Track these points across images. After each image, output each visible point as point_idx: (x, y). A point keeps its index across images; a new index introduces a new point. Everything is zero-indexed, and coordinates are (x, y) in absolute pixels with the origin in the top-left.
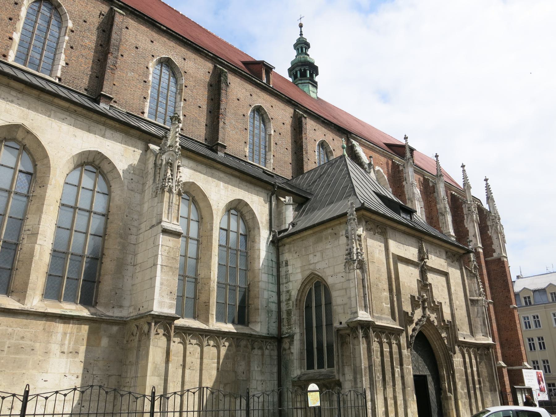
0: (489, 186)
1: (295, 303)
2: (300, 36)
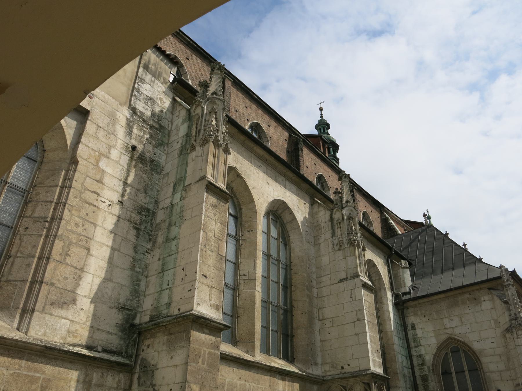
1: (431, 368)
2: (320, 119)
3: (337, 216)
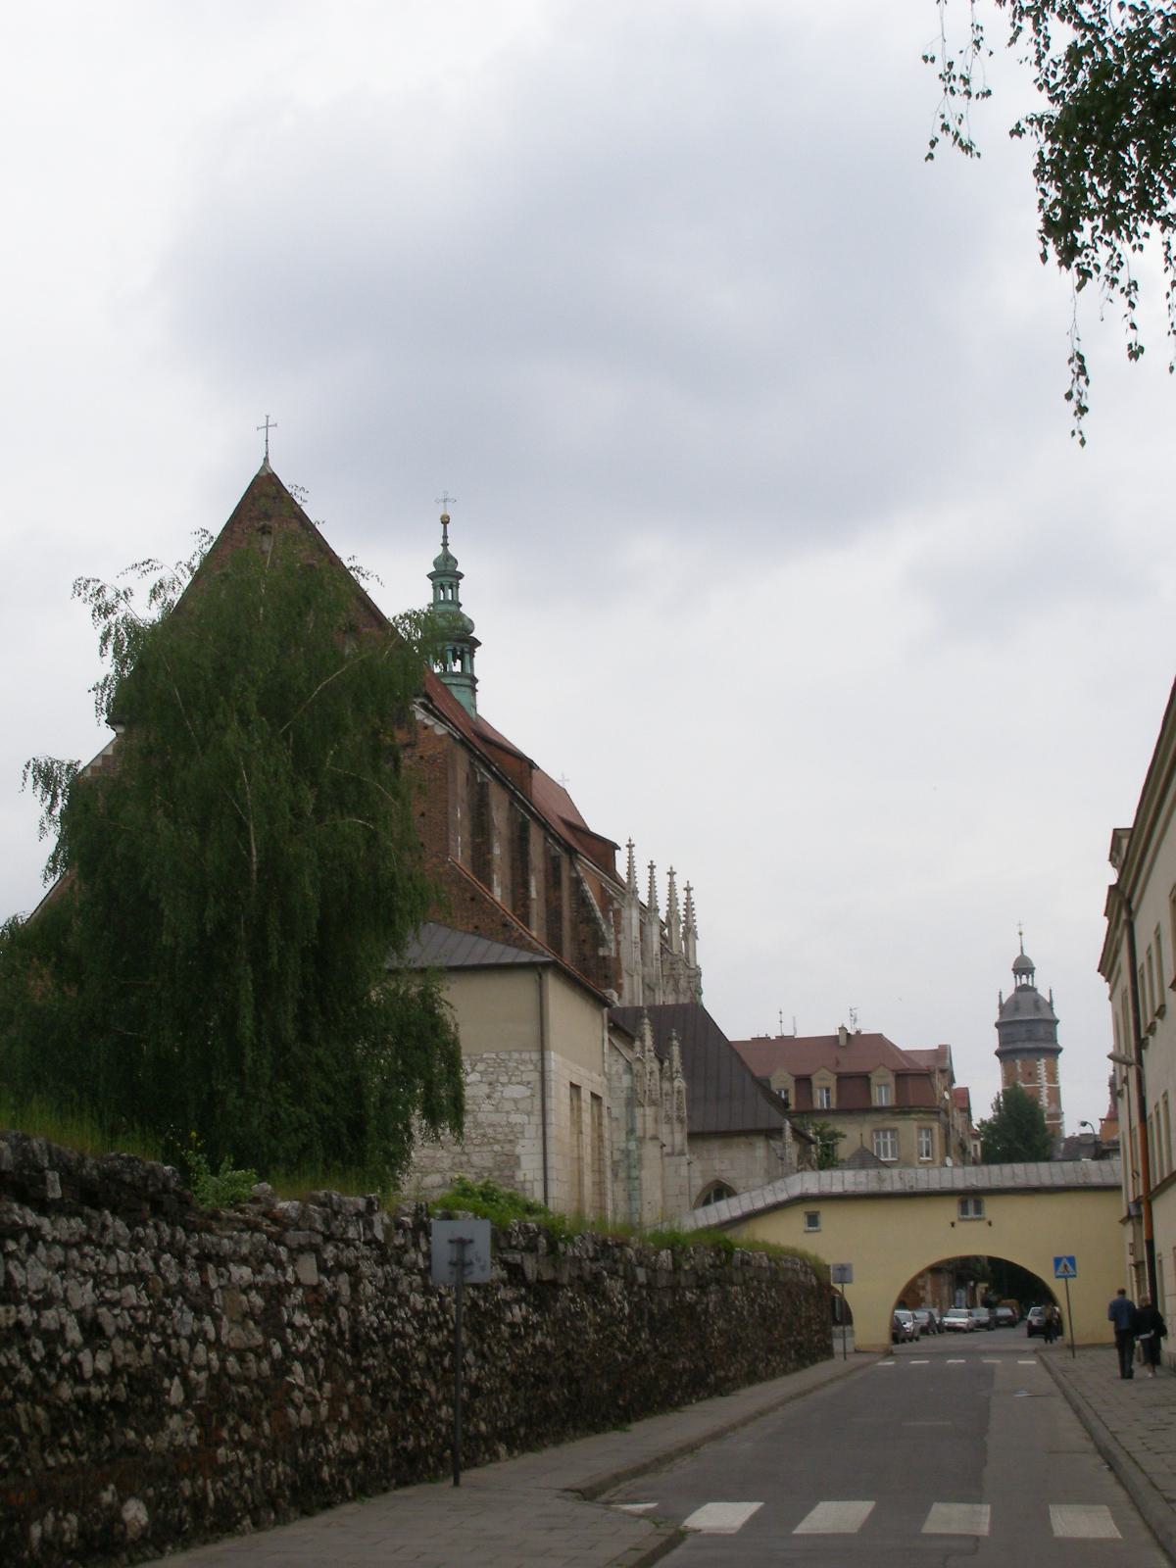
0: (693, 903)
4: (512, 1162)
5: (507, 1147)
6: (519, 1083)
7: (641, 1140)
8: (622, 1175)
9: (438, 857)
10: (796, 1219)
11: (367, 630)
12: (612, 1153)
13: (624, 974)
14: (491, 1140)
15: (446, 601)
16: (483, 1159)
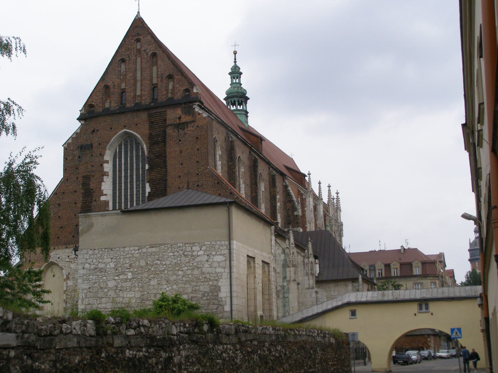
3: (306, 260)
4: (217, 289)
5: (215, 283)
6: (220, 255)
7: (289, 282)
8: (281, 296)
9: (204, 166)
10: (346, 313)
11: (177, 77)
12: (276, 287)
13: (307, 223)
14: (208, 280)
15: (236, 83)
16: (205, 288)
